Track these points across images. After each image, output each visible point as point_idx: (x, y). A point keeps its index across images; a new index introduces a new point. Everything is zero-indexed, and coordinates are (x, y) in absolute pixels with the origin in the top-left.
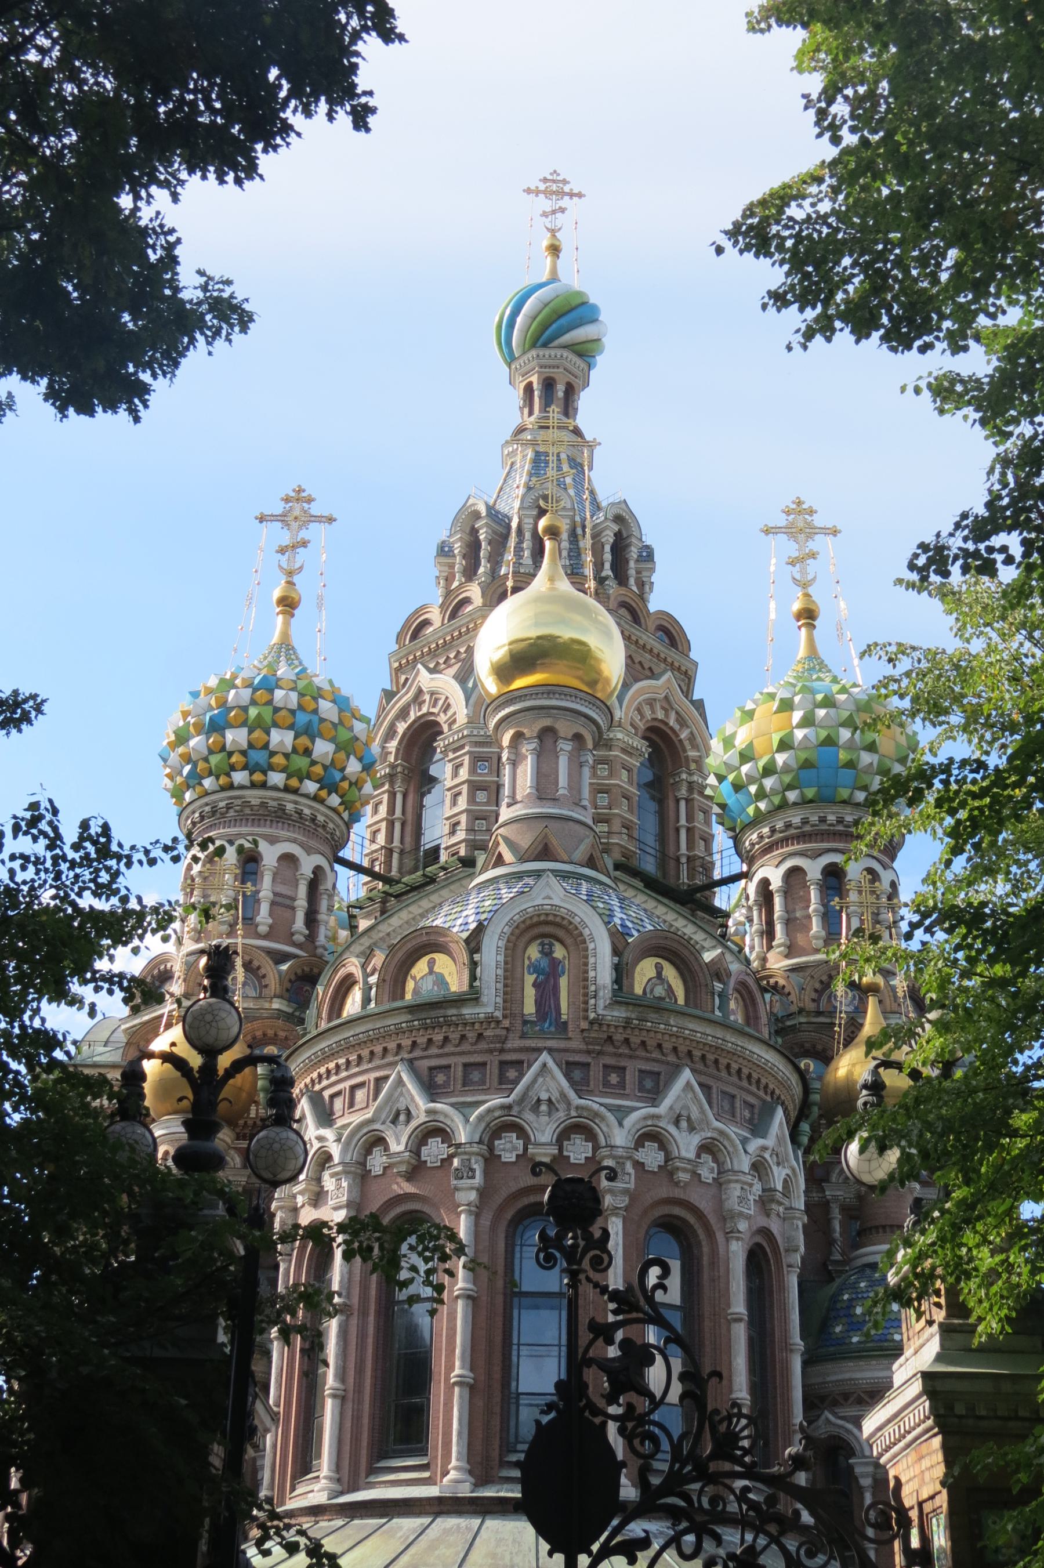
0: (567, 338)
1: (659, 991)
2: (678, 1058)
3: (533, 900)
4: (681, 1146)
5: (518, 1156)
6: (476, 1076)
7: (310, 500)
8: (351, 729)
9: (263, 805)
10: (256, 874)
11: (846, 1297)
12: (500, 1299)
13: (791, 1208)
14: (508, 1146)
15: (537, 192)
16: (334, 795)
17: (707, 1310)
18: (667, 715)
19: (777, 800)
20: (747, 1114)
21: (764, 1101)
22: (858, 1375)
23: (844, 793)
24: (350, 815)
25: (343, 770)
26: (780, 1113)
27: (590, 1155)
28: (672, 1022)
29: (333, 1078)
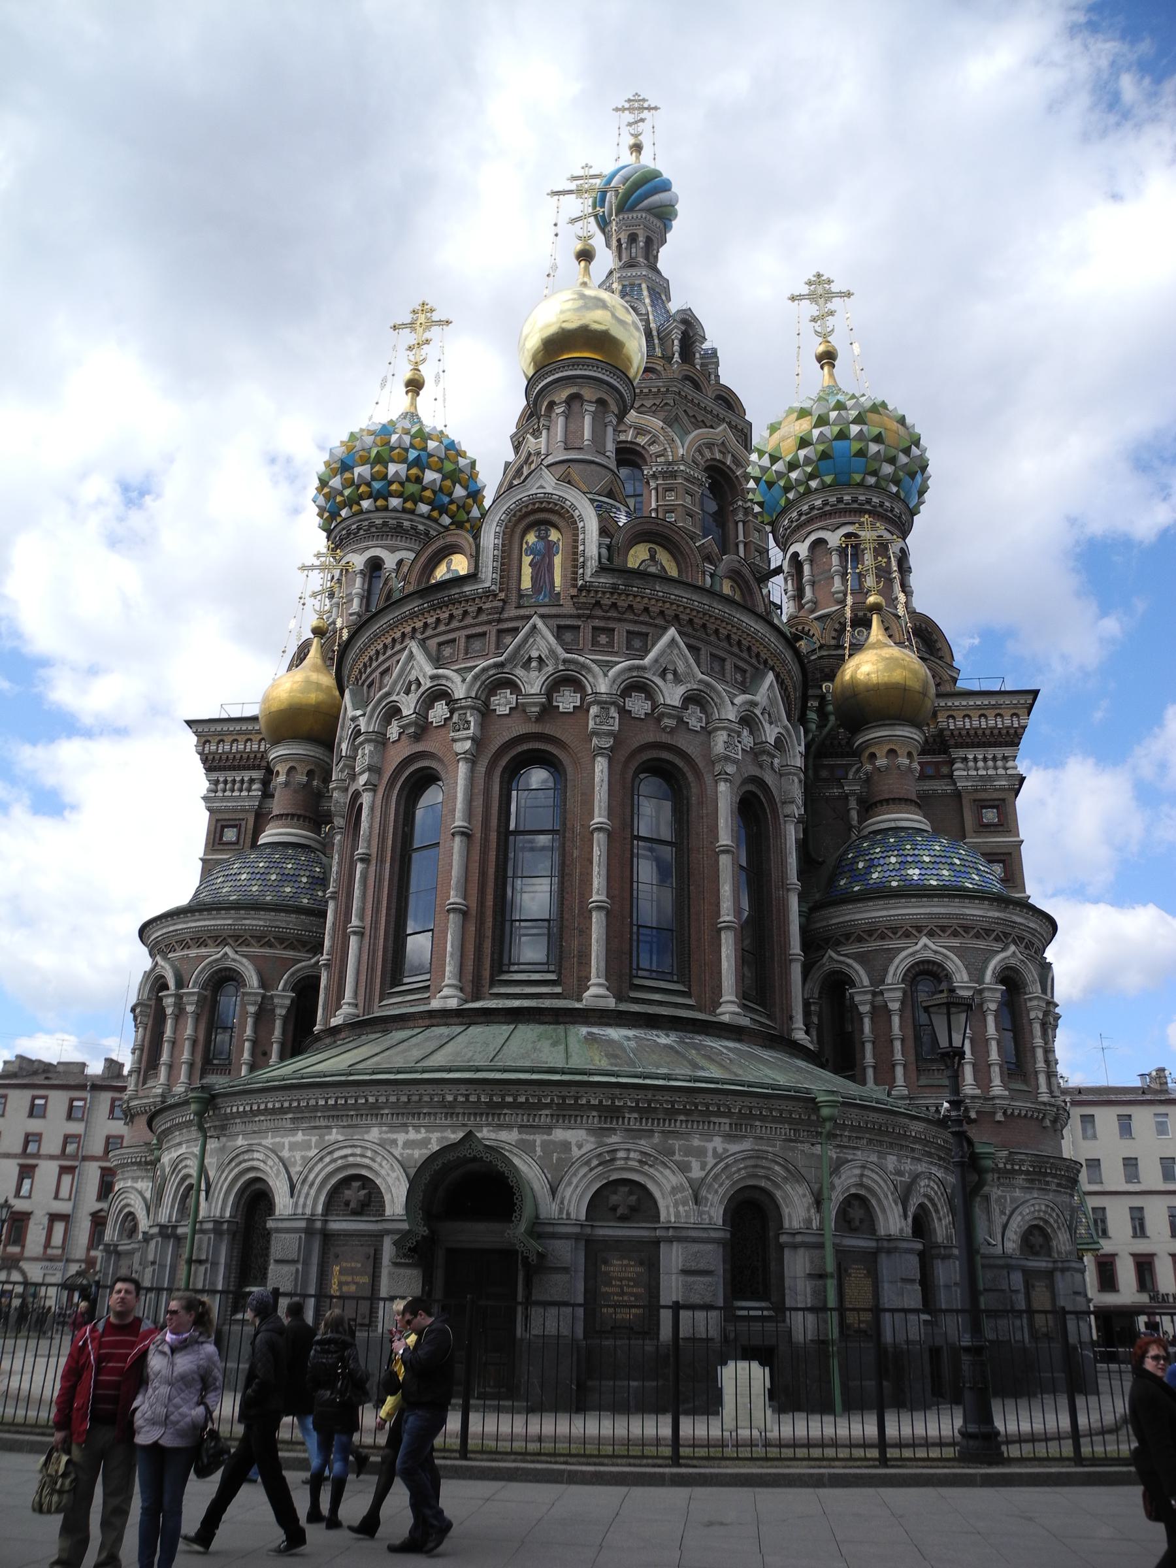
0: (646, 202)
1: (652, 569)
3: (528, 490)
4: (666, 695)
6: (477, 645)
7: (432, 311)
8: (457, 463)
9: (385, 524)
12: (493, 836)
14: (503, 701)
15: (623, 109)
16: (444, 516)
18: (725, 457)
19: (801, 489)
20: (739, 677)
21: (757, 669)
22: (858, 916)
23: (857, 478)
25: (450, 495)
27: (578, 704)
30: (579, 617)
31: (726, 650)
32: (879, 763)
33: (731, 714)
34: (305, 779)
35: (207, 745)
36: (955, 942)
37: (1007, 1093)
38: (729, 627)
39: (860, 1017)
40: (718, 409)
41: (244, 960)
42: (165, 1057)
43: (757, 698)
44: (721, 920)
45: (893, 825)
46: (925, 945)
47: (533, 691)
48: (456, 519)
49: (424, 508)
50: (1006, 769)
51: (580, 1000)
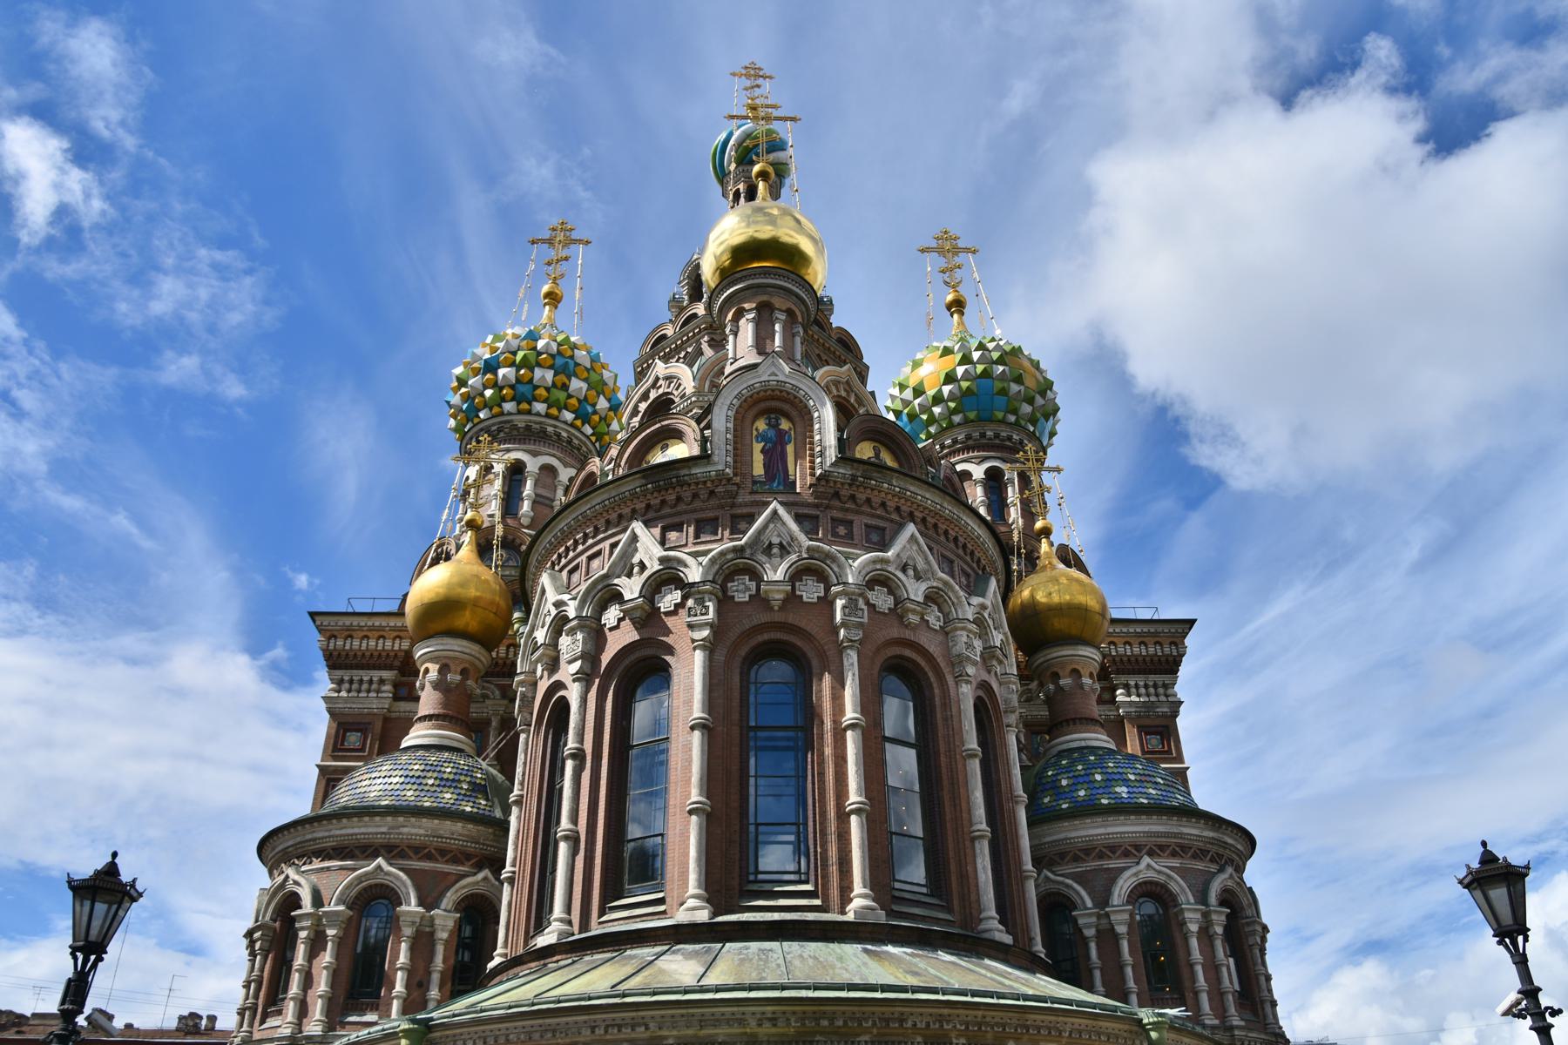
2: (901, 516)
3: (759, 376)
4: (910, 590)
5: (750, 596)
7: (571, 230)
8: (601, 375)
9: (528, 428)
10: (521, 481)
11: (1050, 773)
12: (736, 731)
13: (1006, 674)
14: (741, 587)
16: (587, 426)
17: (942, 747)
20: (965, 582)
21: (977, 574)
22: (1073, 834)
23: (1000, 415)
24: (601, 447)
25: (594, 405)
26: (993, 583)
27: (822, 594)
28: (895, 484)
29: (571, 554)
30: (816, 506)
31: (953, 552)
32: (1062, 682)
33: (970, 614)
34: (458, 677)
35: (332, 641)
36: (1175, 863)
37: (1242, 1023)
38: (957, 529)
39: (1085, 941)
40: (840, 351)
41: (401, 874)
42: (294, 988)
43: (988, 603)
44: (975, 828)
45: (1083, 744)
46: (1149, 866)
47: (776, 578)
48: (598, 430)
49: (568, 416)
50: (1167, 696)
51: (843, 912)
